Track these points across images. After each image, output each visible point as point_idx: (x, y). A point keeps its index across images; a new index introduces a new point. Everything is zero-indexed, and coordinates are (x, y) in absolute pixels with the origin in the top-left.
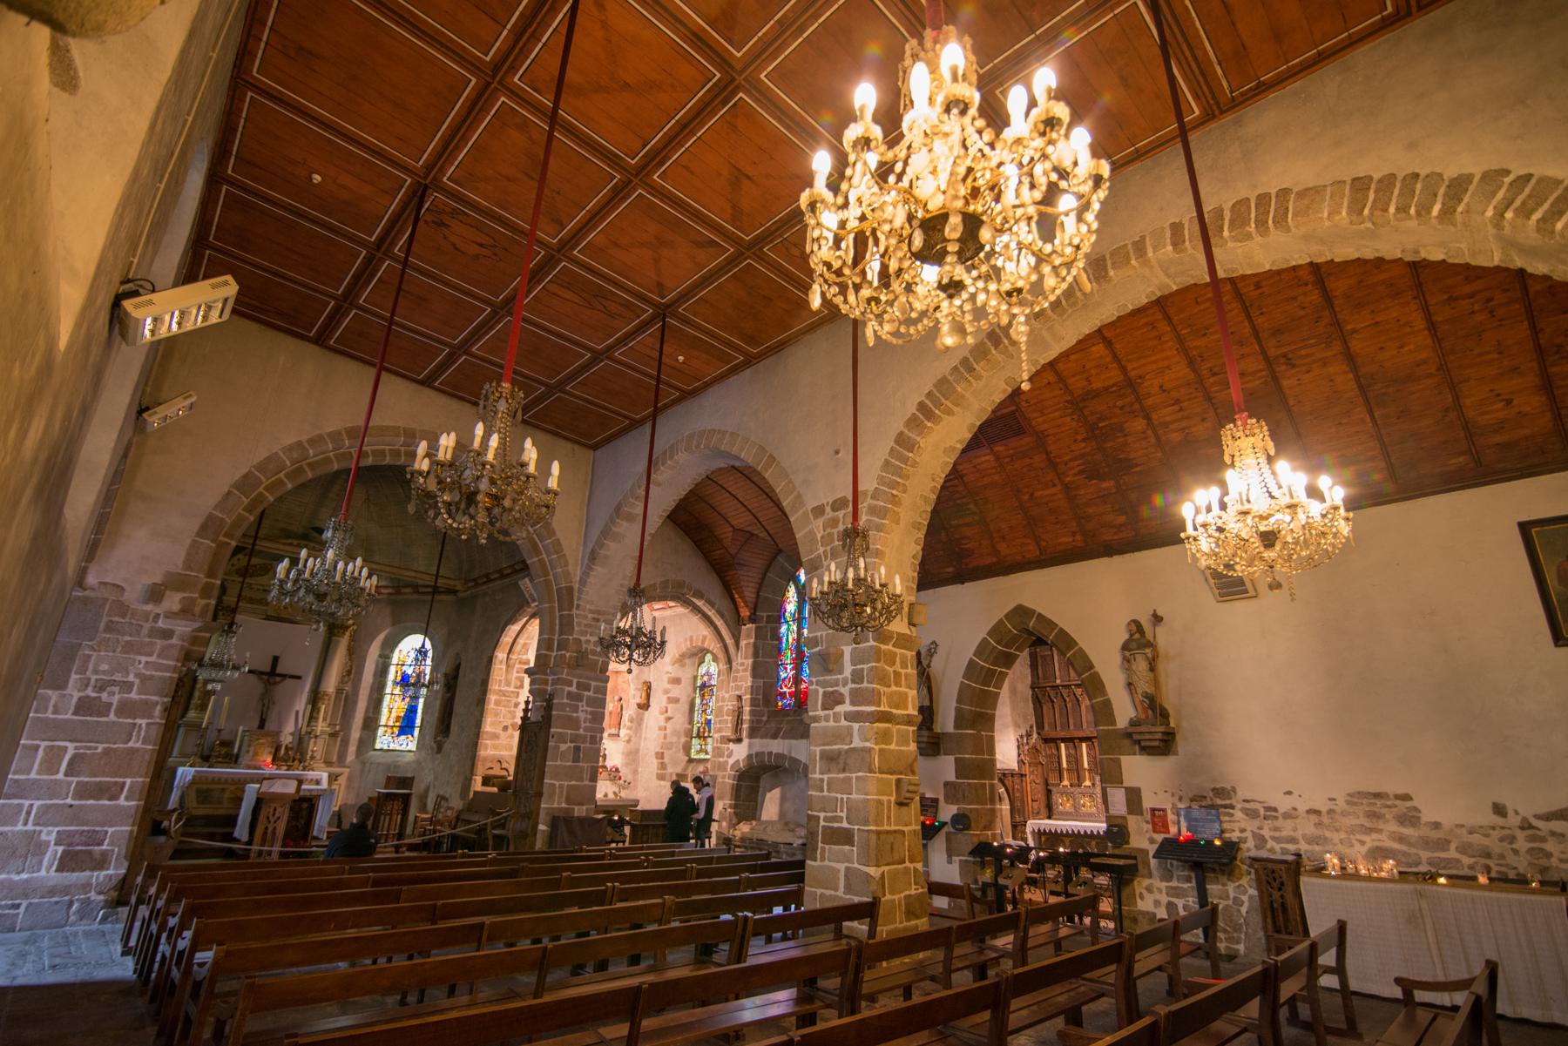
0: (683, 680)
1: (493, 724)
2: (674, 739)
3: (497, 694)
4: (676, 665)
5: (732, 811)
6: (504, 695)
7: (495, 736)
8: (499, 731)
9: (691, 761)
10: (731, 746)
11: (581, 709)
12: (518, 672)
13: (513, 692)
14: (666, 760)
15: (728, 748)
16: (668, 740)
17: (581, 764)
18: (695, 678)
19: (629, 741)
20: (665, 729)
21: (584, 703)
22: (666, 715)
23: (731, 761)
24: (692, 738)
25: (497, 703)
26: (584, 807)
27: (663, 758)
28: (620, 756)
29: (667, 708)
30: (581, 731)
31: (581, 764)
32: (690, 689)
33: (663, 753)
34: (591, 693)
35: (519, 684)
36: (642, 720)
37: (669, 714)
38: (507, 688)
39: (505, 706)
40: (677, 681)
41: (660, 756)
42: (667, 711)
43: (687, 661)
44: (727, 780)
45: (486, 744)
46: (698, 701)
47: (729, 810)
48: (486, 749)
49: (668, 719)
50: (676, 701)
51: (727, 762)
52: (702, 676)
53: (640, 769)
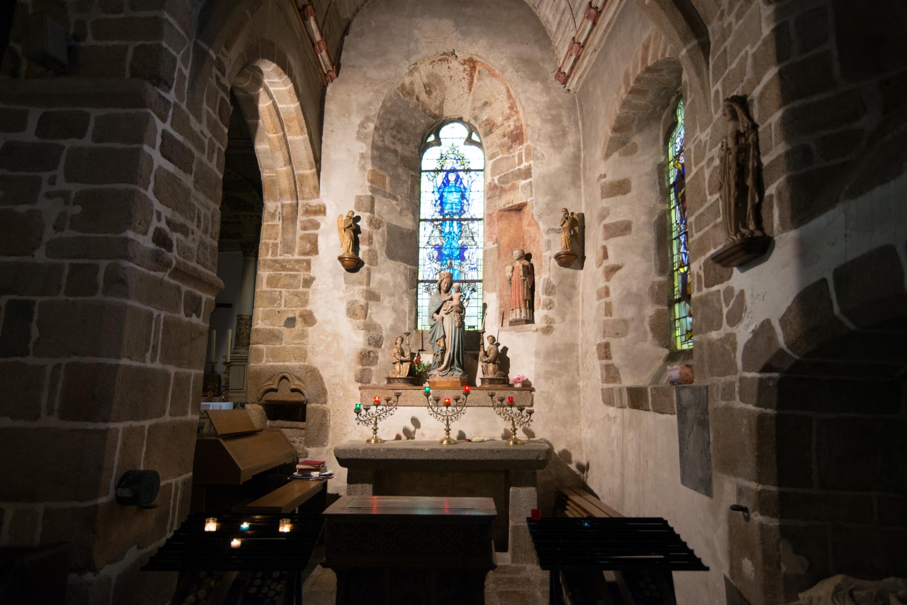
0: (634, 183)
1: (267, 316)
2: (630, 312)
3: (270, 267)
4: (616, 155)
5: (774, 523)
6: (284, 268)
7: (274, 336)
8: (278, 326)
9: (674, 356)
10: (739, 279)
11: (45, 188)
12: (304, 228)
13: (298, 261)
14: (616, 360)
15: (729, 292)
16: (615, 316)
17: (31, 360)
18: (662, 170)
19: (548, 330)
20: (607, 293)
21: (60, 172)
22: (606, 263)
23: (743, 333)
24: (671, 304)
25: (272, 282)
26: (40, 508)
27: (608, 356)
28: (533, 359)
29: (605, 249)
30: (40, 256)
31: (31, 360)
32: (652, 196)
33: (607, 346)
34: (87, 142)
35: (308, 246)
36: (573, 287)
37: (612, 261)
38: (289, 257)
39: (284, 286)
40: (620, 188)
41: (605, 351)
42: (605, 256)
43: (637, 139)
44: (738, 404)
45: (257, 350)
46: (675, 216)
47: (757, 518)
48: (259, 358)
49: (613, 270)
50: (624, 228)
51: (730, 339)
52: (677, 157)
53: (581, 384)
